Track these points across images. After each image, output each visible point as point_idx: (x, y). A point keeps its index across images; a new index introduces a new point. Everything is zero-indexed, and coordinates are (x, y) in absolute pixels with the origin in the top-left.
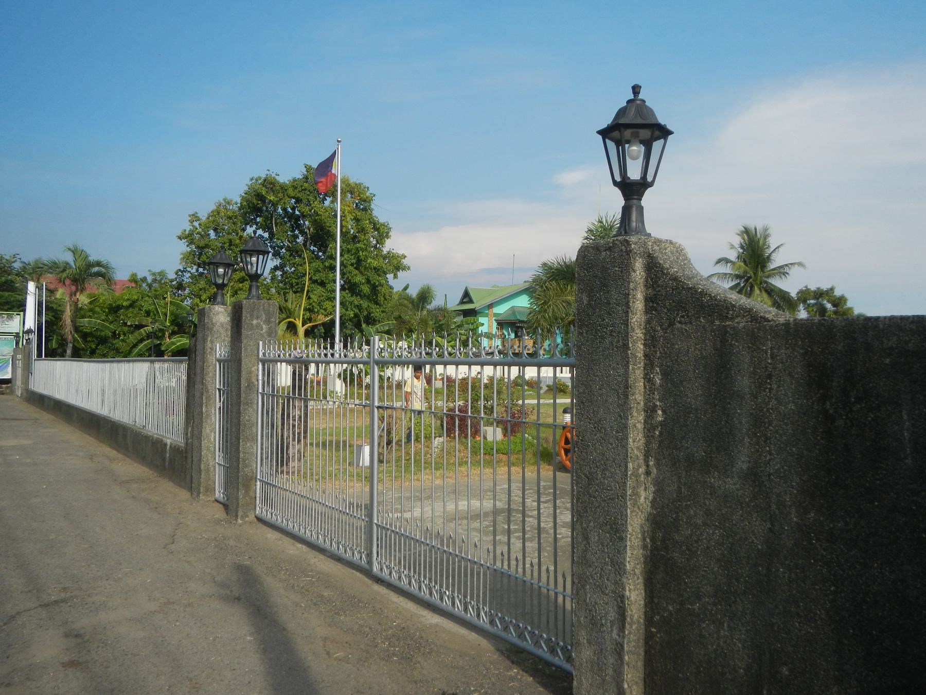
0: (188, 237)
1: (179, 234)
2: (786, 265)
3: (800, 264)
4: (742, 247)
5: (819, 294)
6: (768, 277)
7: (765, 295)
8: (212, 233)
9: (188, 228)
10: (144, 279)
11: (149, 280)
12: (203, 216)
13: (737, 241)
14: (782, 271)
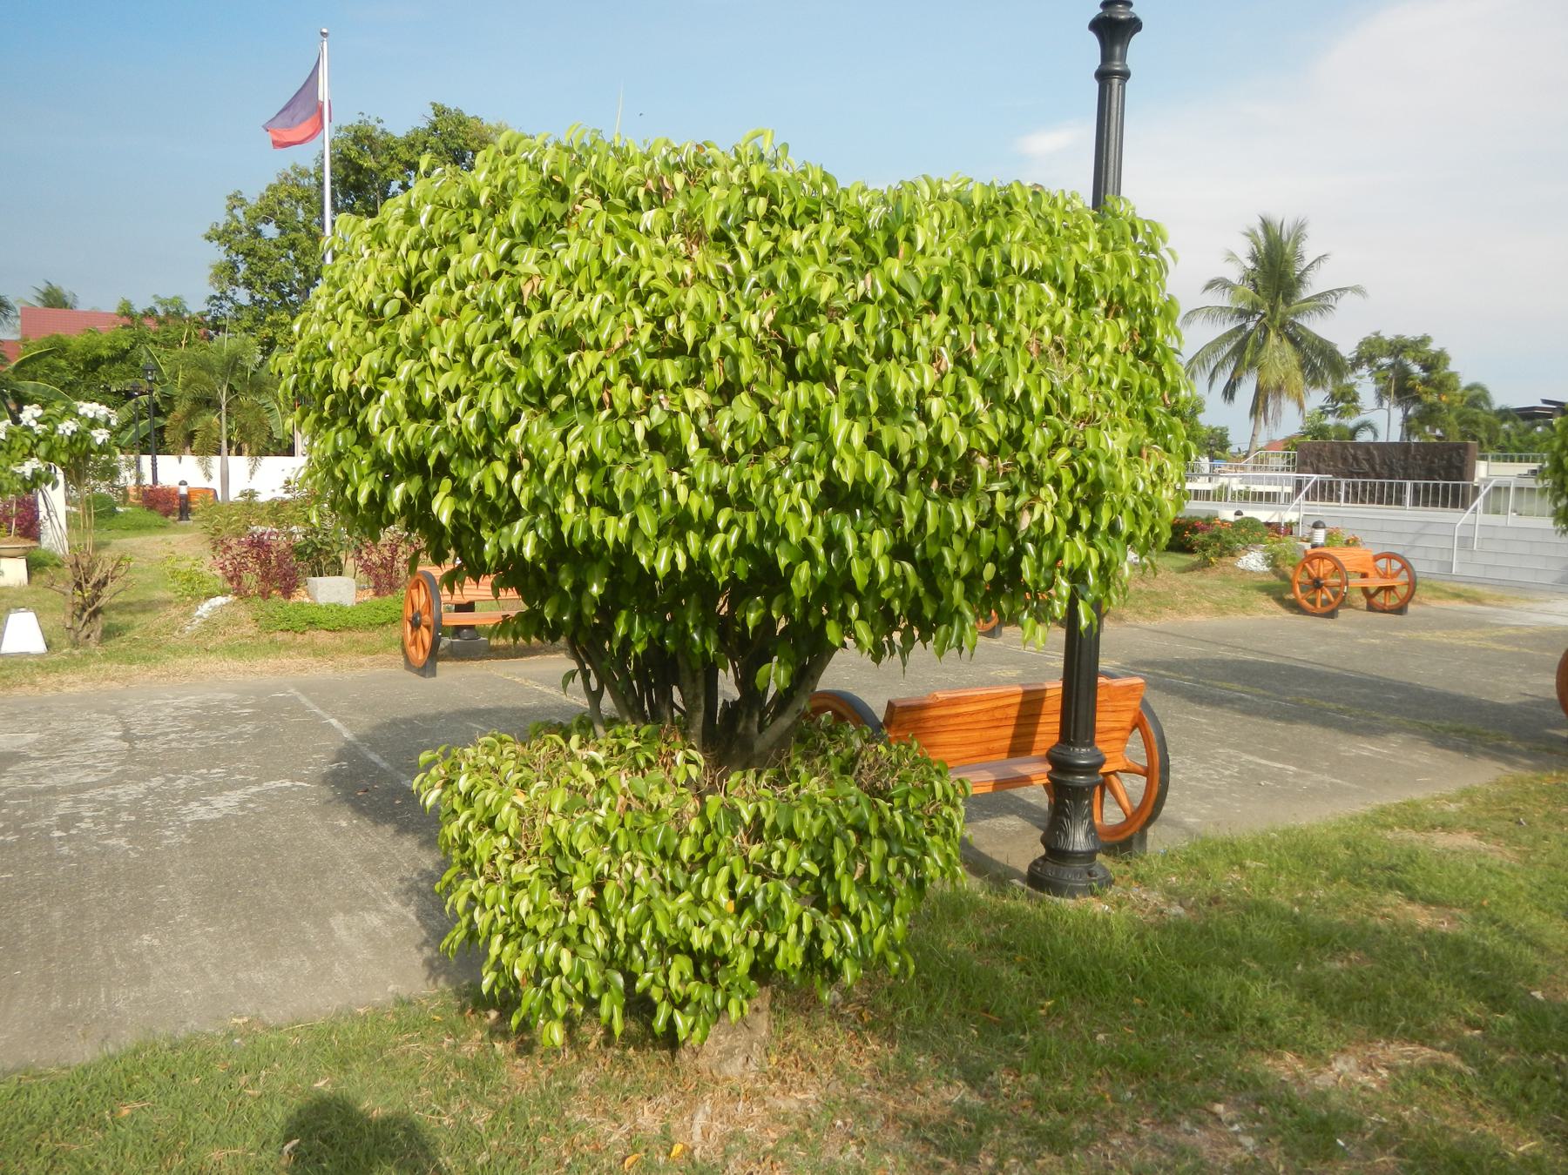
0: (223, 236)
1: (207, 230)
2: (1331, 292)
3: (1357, 290)
4: (1254, 258)
5: (1398, 348)
6: (1296, 314)
7: (1287, 347)
8: (270, 231)
9: (222, 219)
10: (150, 313)
11: (161, 312)
12: (253, 194)
13: (1243, 249)
14: (1322, 303)
